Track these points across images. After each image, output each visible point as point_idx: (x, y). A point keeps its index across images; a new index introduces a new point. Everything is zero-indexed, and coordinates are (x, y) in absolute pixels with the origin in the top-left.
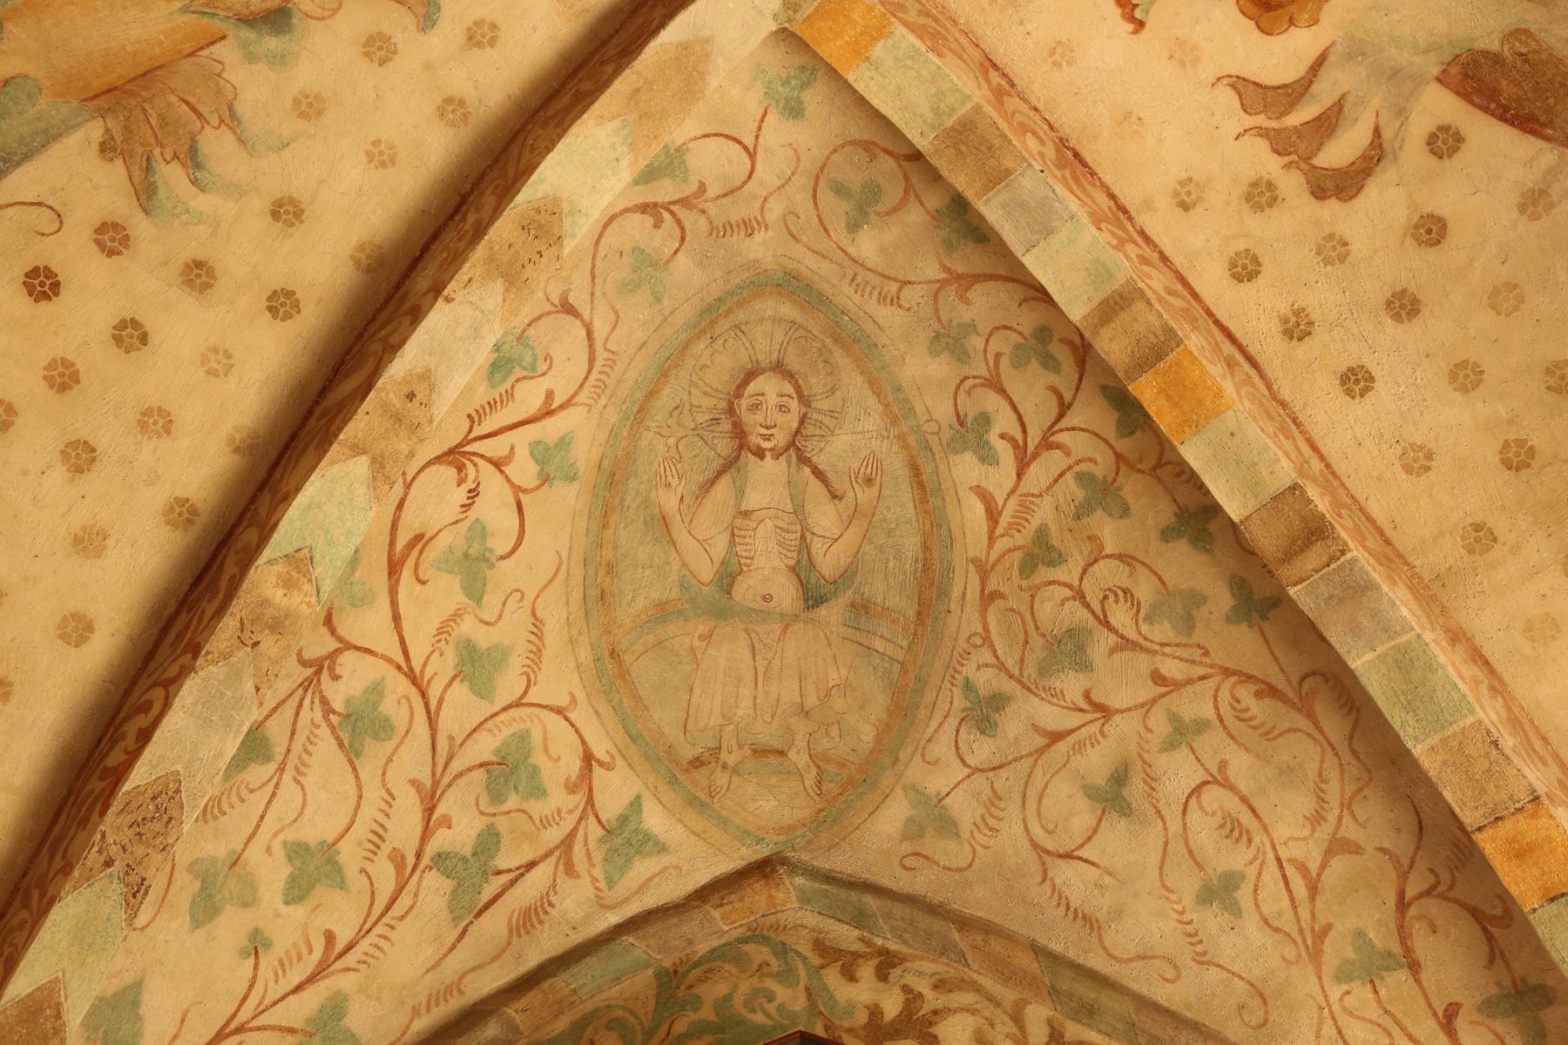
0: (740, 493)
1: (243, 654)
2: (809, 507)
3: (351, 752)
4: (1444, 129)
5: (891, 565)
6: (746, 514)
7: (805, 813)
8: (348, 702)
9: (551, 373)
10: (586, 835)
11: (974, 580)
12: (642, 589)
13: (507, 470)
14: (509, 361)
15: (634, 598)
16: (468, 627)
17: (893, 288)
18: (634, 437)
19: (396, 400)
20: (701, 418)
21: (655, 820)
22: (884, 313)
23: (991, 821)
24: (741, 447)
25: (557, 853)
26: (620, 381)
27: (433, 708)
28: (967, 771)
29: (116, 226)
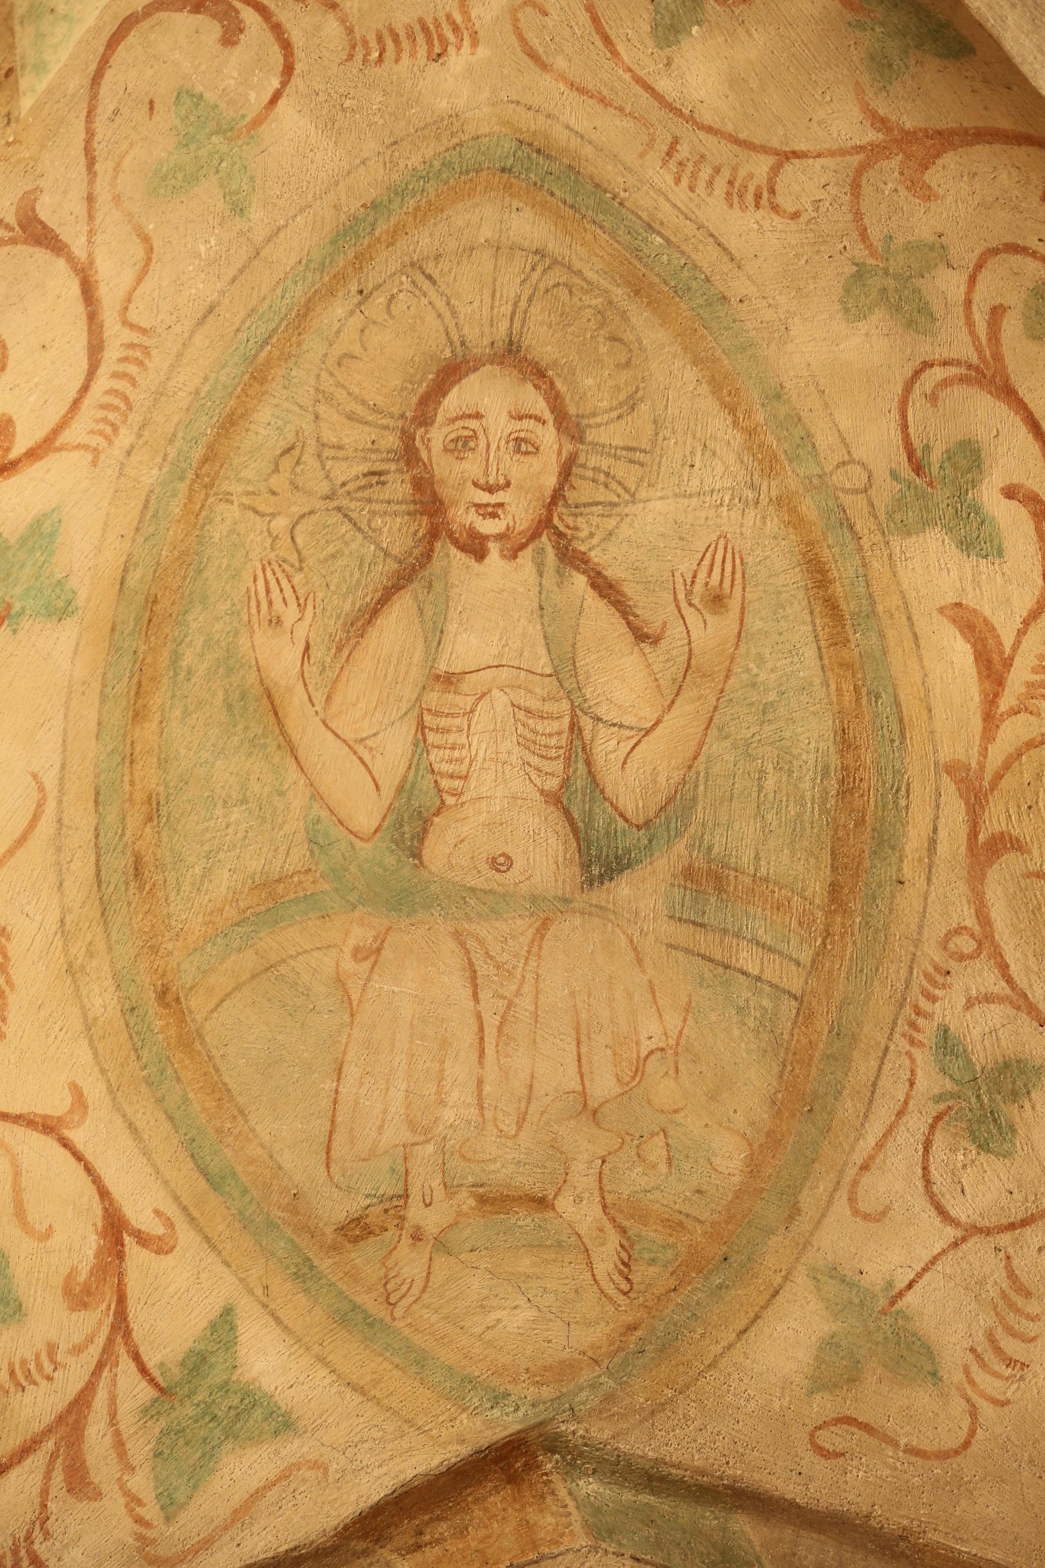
0: (435, 636)
2: (586, 661)
5: (770, 783)
6: (449, 681)
7: (595, 1335)
10: (113, 1400)
11: (954, 813)
12: (222, 855)
15: (207, 873)
17: (760, 167)
18: (195, 518)
20: (345, 472)
21: (265, 1359)
22: (742, 227)
23: (1011, 1347)
24: (434, 534)
25: (50, 1445)
26: (159, 395)
28: (951, 1233)
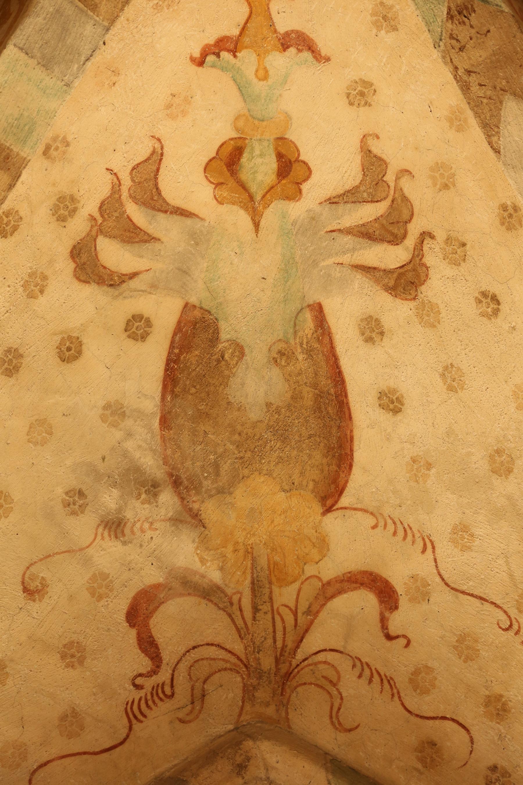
4: (148, 323)
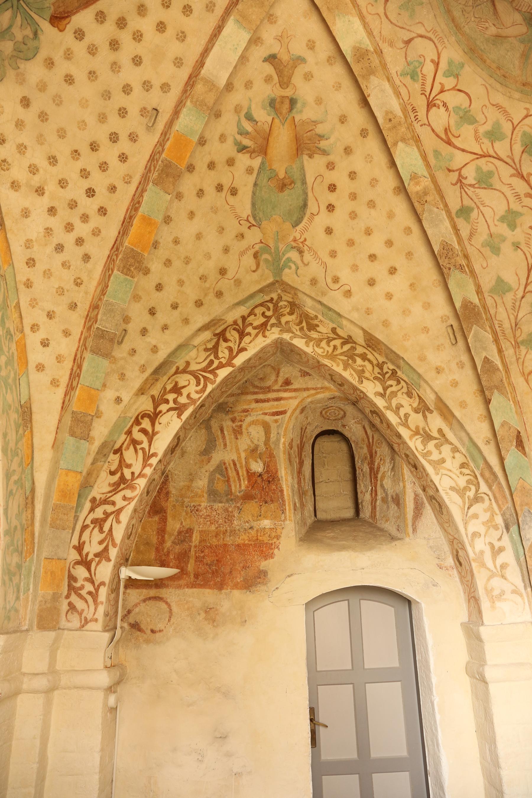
1: (426, 206)
3: (490, 187)
8: (475, 179)
9: (426, 57)
13: (446, 89)
14: (413, 71)
16: (482, 130)
19: (389, 125)
27: (495, 156)
29: (328, 164)
